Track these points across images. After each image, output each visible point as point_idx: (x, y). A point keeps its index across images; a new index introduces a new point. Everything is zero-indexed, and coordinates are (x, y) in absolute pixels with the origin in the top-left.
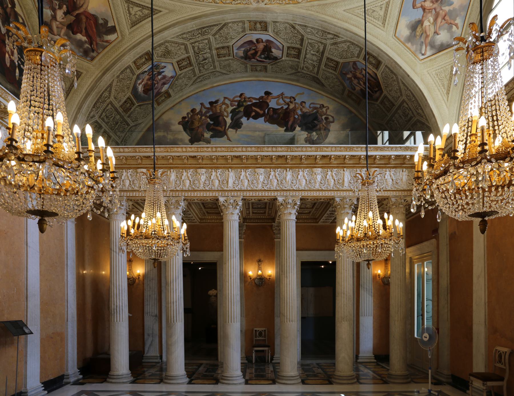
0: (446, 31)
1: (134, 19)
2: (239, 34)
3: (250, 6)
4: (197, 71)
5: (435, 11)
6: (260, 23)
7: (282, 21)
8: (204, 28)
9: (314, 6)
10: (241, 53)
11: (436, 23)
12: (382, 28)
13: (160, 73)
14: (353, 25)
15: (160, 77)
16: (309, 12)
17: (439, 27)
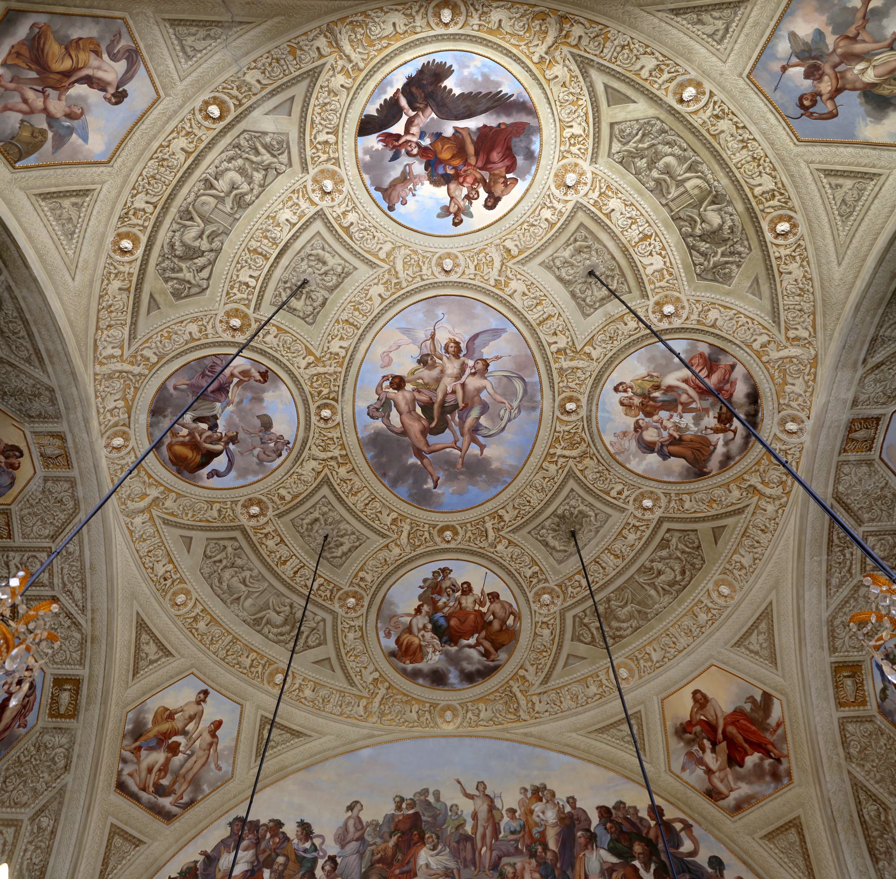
0: (885, 22)
1: (766, 653)
2: (876, 472)
3: (805, 446)
5: (839, 64)
6: (850, 430)
7: (853, 390)
8: (830, 541)
9: (825, 325)
11: (868, 53)
12: (883, 178)
14: (872, 245)
16: (836, 334)
17: (876, 42)
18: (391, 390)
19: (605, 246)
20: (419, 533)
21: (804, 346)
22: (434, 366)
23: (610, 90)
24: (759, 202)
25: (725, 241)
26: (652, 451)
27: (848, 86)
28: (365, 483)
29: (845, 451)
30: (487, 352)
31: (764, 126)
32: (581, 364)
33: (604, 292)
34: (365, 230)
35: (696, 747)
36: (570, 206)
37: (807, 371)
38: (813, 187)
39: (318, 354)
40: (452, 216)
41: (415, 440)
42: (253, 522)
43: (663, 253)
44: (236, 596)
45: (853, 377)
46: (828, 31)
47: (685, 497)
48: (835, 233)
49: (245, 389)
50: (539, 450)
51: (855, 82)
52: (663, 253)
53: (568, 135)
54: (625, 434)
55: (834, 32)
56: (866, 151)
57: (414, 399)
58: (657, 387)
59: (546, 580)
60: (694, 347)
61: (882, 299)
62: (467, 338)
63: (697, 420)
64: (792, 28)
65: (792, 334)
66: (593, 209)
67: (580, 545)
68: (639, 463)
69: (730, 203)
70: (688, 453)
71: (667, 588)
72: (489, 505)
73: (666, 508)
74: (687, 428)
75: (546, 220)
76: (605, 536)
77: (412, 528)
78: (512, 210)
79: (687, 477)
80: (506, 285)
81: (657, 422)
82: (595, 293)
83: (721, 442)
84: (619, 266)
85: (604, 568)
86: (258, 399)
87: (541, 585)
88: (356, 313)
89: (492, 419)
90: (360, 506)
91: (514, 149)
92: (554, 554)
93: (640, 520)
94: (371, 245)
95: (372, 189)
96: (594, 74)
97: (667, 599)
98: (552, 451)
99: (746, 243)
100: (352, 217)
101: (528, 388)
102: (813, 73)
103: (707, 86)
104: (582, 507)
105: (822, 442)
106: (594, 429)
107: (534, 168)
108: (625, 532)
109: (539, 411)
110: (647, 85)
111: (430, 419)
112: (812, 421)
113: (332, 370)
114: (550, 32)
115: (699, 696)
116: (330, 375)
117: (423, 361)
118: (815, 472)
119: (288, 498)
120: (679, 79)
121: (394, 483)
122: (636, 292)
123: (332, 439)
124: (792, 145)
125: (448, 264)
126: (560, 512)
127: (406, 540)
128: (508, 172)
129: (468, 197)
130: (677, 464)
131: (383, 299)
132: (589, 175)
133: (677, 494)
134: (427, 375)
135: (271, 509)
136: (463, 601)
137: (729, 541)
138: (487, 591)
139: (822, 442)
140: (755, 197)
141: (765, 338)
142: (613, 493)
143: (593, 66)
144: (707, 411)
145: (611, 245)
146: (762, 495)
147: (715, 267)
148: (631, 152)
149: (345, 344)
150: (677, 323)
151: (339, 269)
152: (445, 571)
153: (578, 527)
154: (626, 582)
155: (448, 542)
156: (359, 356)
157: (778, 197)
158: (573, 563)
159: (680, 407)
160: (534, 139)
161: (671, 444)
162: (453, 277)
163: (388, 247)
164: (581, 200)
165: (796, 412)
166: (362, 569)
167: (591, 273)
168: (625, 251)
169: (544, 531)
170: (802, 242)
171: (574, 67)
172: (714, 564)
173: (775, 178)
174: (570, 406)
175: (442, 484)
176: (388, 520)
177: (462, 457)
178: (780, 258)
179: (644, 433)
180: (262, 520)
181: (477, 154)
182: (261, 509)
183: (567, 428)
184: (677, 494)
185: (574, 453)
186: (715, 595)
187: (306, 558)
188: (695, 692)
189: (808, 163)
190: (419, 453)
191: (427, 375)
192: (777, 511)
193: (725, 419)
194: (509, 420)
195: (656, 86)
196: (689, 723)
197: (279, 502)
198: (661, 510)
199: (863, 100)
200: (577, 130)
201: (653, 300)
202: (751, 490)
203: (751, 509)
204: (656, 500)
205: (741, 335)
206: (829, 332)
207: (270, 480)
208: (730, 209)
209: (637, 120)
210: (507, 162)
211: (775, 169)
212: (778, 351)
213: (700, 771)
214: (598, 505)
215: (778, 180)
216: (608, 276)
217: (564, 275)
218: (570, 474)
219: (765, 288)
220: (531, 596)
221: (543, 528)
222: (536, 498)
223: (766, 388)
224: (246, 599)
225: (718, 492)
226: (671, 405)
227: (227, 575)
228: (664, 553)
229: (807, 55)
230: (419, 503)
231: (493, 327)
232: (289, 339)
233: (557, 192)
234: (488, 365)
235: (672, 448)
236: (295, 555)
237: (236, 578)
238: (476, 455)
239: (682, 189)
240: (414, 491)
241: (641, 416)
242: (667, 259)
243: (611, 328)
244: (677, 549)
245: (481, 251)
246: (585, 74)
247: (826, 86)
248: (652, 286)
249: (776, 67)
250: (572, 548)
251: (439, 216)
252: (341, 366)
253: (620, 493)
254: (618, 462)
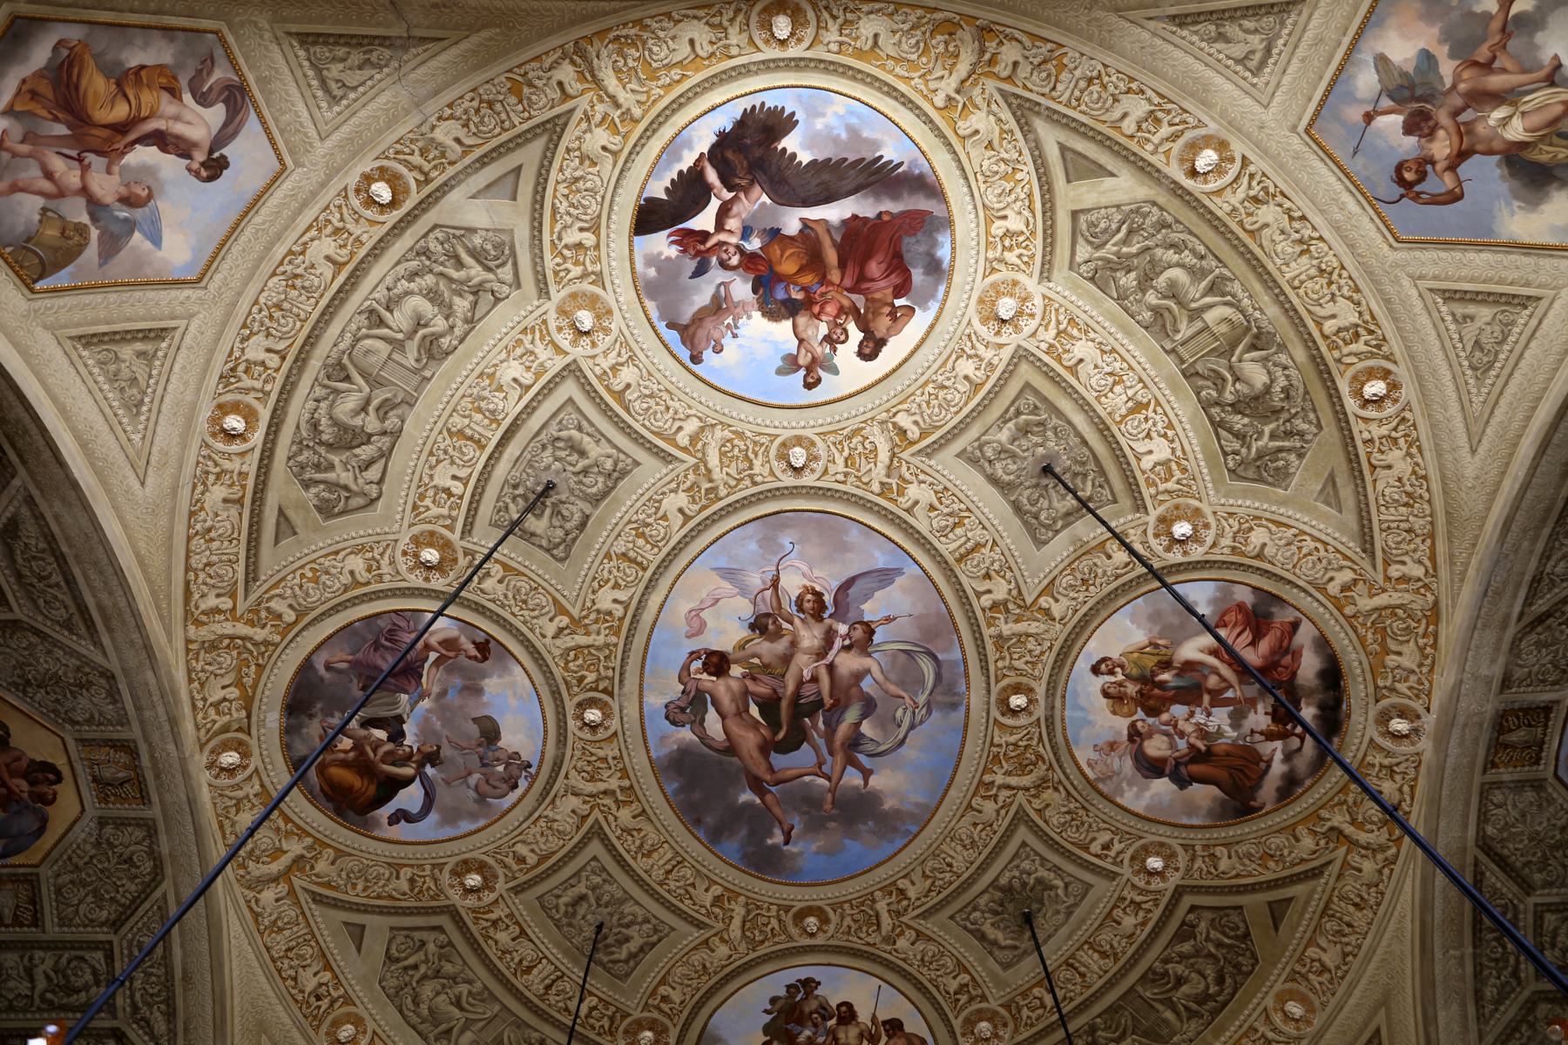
0: (1539, 37)
3: (1424, 758)
5: (1463, 109)
7: (1502, 660)
9: (1451, 556)
11: (1512, 90)
16: (1471, 572)
17: (1524, 71)
18: (705, 676)
19: (1069, 423)
20: (765, 920)
21: (1417, 591)
22: (777, 634)
23: (1069, 155)
24: (1333, 347)
25: (1277, 412)
26: (1160, 775)
27: (1479, 147)
28: (665, 837)
29: (1494, 765)
30: (871, 610)
31: (1338, 216)
32: (1034, 627)
33: (1071, 502)
34: (651, 396)
36: (1006, 354)
37: (1421, 630)
38: (1424, 319)
39: (575, 612)
40: (802, 372)
41: (750, 763)
42: (471, 901)
43: (1170, 433)
44: (443, 1027)
45: (1500, 640)
46: (1441, 52)
47: (1220, 851)
48: (1465, 398)
49: (449, 671)
50: (966, 777)
51: (1491, 140)
52: (1170, 433)
53: (1000, 232)
54: (1112, 746)
55: (1452, 56)
56: (1513, 257)
57: (746, 693)
58: (1166, 665)
59: (984, 998)
60: (1227, 594)
61: (1548, 510)
62: (835, 585)
63: (1237, 719)
64: (1380, 49)
65: (1395, 571)
66: (1046, 358)
67: (1041, 936)
68: (1138, 796)
69: (1282, 347)
70: (1223, 775)
71: (1194, 1006)
72: (881, 873)
73: (1188, 870)
74: (1219, 733)
75: (966, 377)
76: (1083, 921)
77: (748, 912)
78: (905, 360)
79: (1222, 816)
80: (901, 492)
81: (1167, 724)
82: (1056, 504)
83: (1279, 756)
84: (1095, 456)
85: (1083, 975)
86: (478, 691)
87: (975, 1006)
88: (641, 542)
89: (882, 725)
90: (658, 874)
91: (907, 257)
92: (997, 953)
93: (1142, 892)
94: (664, 422)
95: (661, 326)
96: (1041, 127)
97: (1194, 1025)
98: (987, 778)
99: (1312, 416)
100: (628, 374)
101: (944, 671)
102: (1418, 124)
103: (1238, 148)
104: (1042, 873)
105: (1453, 750)
106: (1060, 738)
107: (942, 289)
108: (1118, 913)
109: (963, 709)
110: (1133, 145)
111: (774, 725)
112: (1433, 716)
113: (600, 640)
114: (963, 56)
116: (599, 649)
117: (761, 625)
118: (1444, 803)
119: (532, 859)
120: (1188, 135)
121: (715, 837)
122: (1125, 502)
123: (605, 760)
124: (1386, 247)
125: (798, 456)
126: (1003, 881)
127: (738, 933)
128: (897, 296)
129: (828, 339)
130: (1204, 794)
131: (687, 518)
132: (1038, 301)
133: (1206, 847)
134: (767, 649)
135: (501, 879)
136: (841, 1035)
137: (1298, 924)
138: (881, 1017)
139: (1453, 750)
140: (1325, 337)
141: (1348, 576)
142: (1095, 848)
143: (1038, 114)
144: (1252, 703)
145: (1079, 420)
146: (1356, 843)
147: (1260, 456)
148: (1109, 261)
149: (622, 596)
150: (1197, 552)
151: (609, 465)
152: (809, 985)
153: (1035, 906)
154: (1122, 998)
155: (812, 935)
156: (647, 617)
157: (1365, 337)
158: (1028, 969)
159: (1206, 698)
160: (940, 238)
161: (1193, 761)
162: (808, 480)
163: (692, 426)
164: (1024, 344)
165: (1406, 701)
166: (663, 982)
167: (1047, 470)
168: (1103, 430)
169: (977, 914)
170: (1407, 415)
171: (1006, 115)
172: (1274, 965)
173: (1358, 304)
174: (1018, 701)
175: (799, 837)
176: (708, 899)
177: (832, 791)
178: (1371, 441)
179: (1146, 743)
180: (488, 897)
181: (842, 265)
182: (485, 878)
183: (1012, 739)
184: (1206, 847)
185: (1026, 781)
186: (1277, 1018)
187: (565, 964)
189: (1415, 279)
190: (757, 785)
191: (767, 649)
192: (1380, 872)
193: (1285, 716)
194: (912, 727)
195: (1149, 147)
197: (515, 867)
198: (1178, 875)
199: (1506, 172)
200: (1015, 223)
201: (1154, 514)
202: (1334, 836)
203: (1335, 869)
204: (1169, 857)
205: (1308, 571)
206: (1458, 568)
207: (498, 830)
208: (1283, 358)
209: (1118, 206)
210: (895, 279)
211: (1357, 290)
212: (1371, 596)
214: (1070, 868)
215: (1364, 308)
216: (1076, 475)
217: (1000, 472)
218: (1021, 817)
219: (1347, 493)
220: (957, 1024)
221: (975, 909)
222: (961, 859)
223: (1353, 660)
224: (462, 1032)
225: (1276, 841)
226: (1191, 694)
227: (427, 990)
228: (1186, 947)
229: (1407, 93)
230: (759, 869)
231: (880, 565)
232: (524, 586)
233: (983, 331)
234: (873, 632)
235: (1194, 768)
236: (545, 959)
237: (443, 997)
238: (857, 788)
239: (1198, 325)
240: (751, 849)
241: (1140, 714)
242: (1176, 445)
243: (1084, 564)
244: (1208, 939)
245: (856, 432)
246: (1026, 128)
247: (1441, 148)
248: (1153, 491)
249: (1355, 114)
250: (1027, 944)
251: (780, 372)
252: (617, 634)
253: (1106, 847)
254: (1102, 794)
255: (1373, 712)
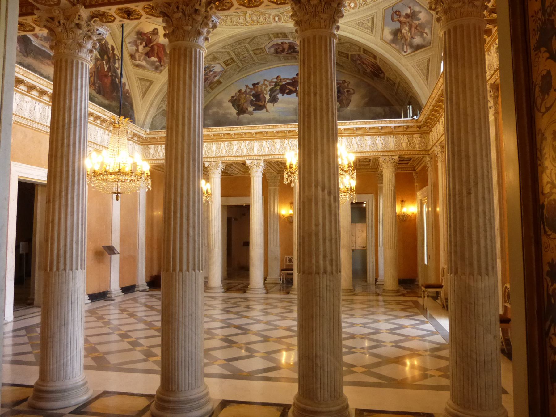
4: (240, 65)
10: (272, 50)
13: (211, 71)
15: (211, 73)
35: (140, 42)
46: (420, 22)
55: (419, 24)
102: (407, 16)
115: (156, 31)
146: (245, 17)
188: (156, 29)
189: (377, 12)
196: (145, 34)
203: (237, 14)
213: (134, 48)
247: (402, 19)
249: (411, 5)
255: (277, 13)
